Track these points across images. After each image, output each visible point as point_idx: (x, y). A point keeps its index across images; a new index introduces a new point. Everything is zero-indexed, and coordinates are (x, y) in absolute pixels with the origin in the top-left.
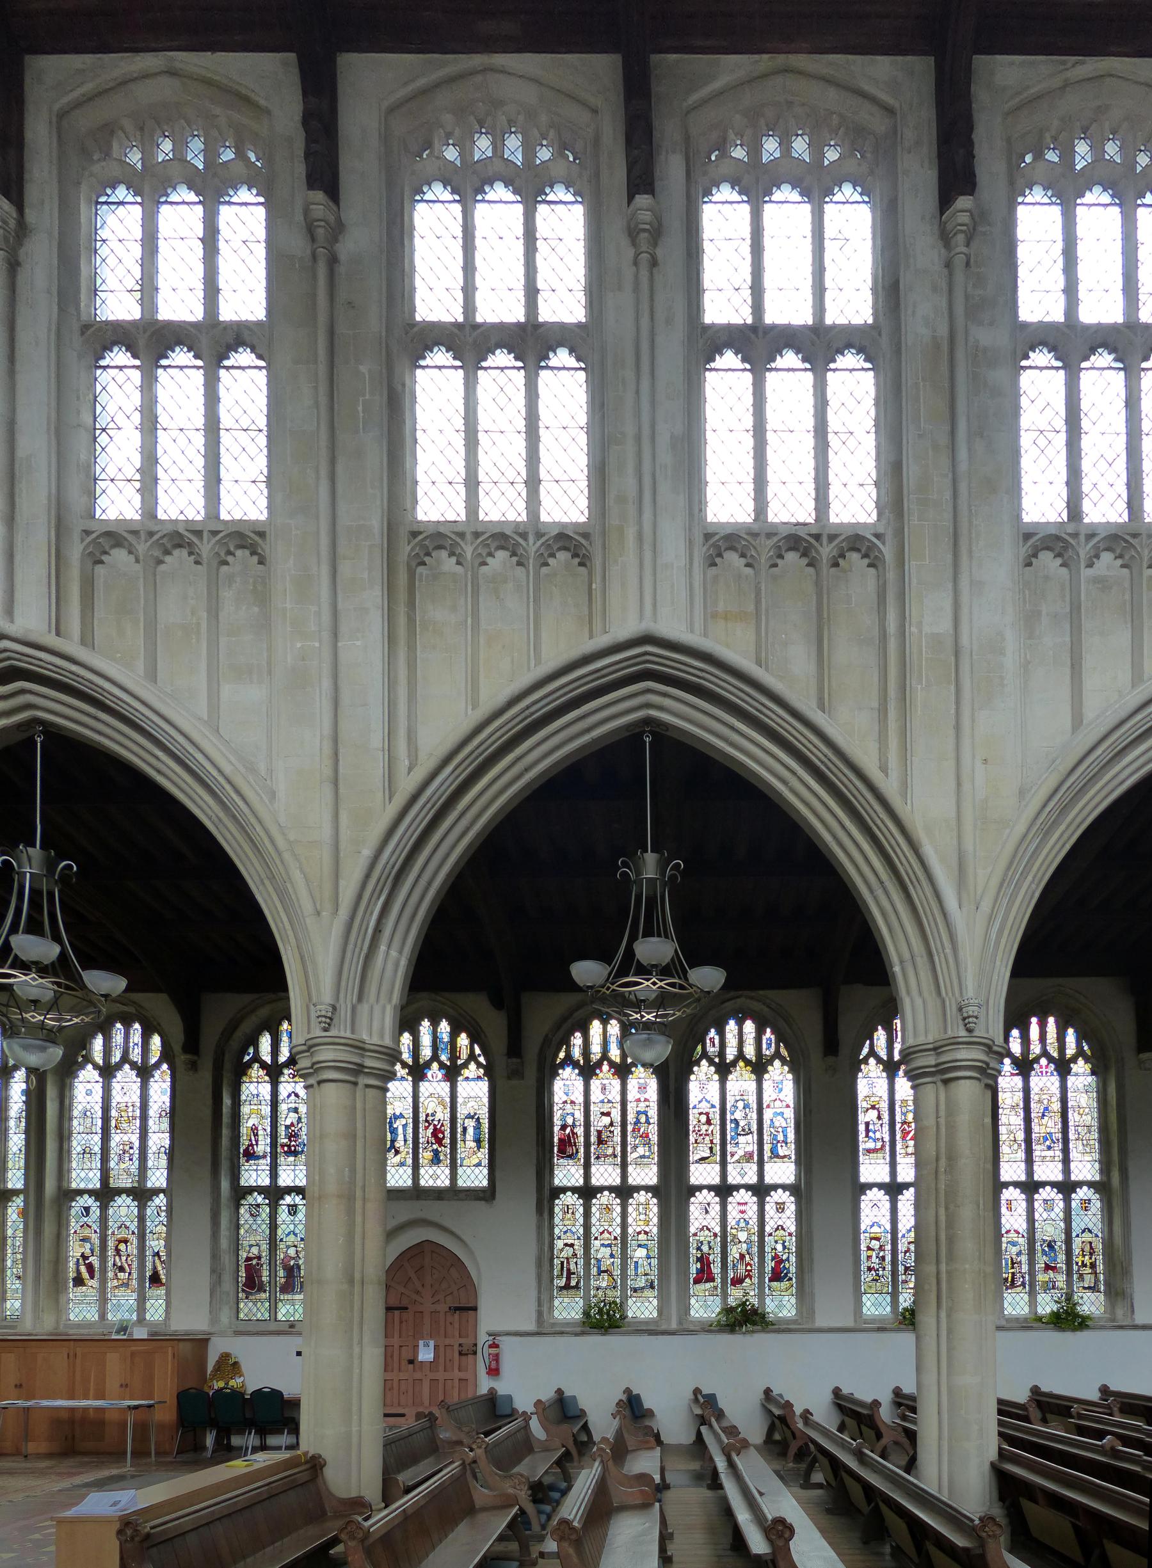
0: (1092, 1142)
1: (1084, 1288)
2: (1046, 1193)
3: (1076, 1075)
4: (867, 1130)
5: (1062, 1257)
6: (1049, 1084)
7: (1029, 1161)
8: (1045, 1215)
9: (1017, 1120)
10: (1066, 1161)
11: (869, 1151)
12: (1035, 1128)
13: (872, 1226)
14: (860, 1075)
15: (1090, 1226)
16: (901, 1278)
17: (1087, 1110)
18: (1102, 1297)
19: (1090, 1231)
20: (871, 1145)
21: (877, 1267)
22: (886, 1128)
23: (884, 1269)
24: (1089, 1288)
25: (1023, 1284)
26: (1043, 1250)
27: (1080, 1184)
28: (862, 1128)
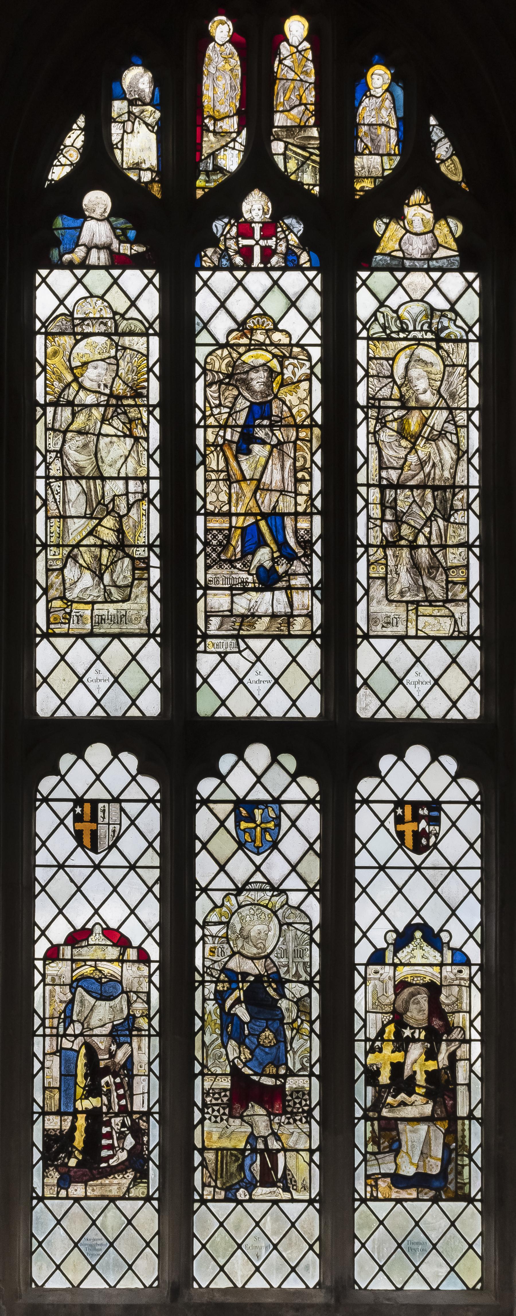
0: (454, 557)
1: (398, 1181)
2: (247, 772)
3: (399, 265)
5: (306, 1048)
6: (274, 305)
7: (180, 638)
8: (241, 867)
9: (129, 458)
10: (339, 639)
12: (210, 491)
15: (434, 916)
17: (439, 418)
18: (472, 1221)
19: (433, 938)
24: (420, 1181)
25: (137, 1163)
26: (227, 1017)
27: (397, 735)
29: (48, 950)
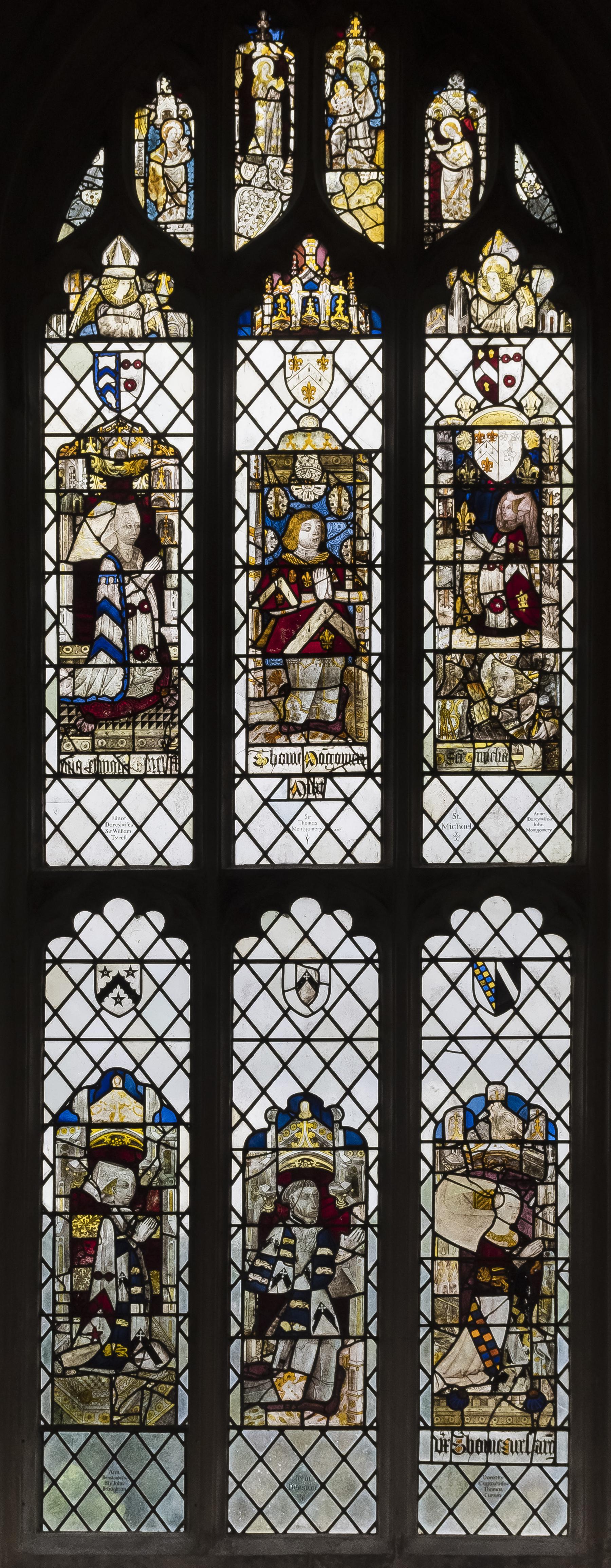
4: (87, 607)
11: (92, 711)
13: (98, 1092)
14: (58, 325)
16: (244, 1351)
20: (103, 680)
21: (117, 1294)
22: (182, 596)
23: (154, 1307)
28: (57, 592)
29: (249, 1138)
